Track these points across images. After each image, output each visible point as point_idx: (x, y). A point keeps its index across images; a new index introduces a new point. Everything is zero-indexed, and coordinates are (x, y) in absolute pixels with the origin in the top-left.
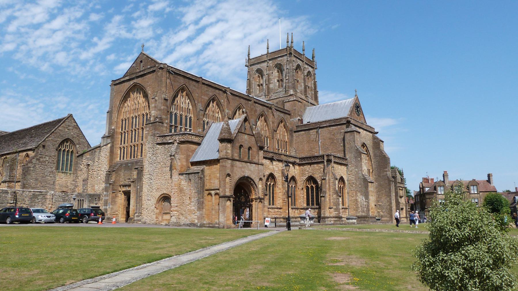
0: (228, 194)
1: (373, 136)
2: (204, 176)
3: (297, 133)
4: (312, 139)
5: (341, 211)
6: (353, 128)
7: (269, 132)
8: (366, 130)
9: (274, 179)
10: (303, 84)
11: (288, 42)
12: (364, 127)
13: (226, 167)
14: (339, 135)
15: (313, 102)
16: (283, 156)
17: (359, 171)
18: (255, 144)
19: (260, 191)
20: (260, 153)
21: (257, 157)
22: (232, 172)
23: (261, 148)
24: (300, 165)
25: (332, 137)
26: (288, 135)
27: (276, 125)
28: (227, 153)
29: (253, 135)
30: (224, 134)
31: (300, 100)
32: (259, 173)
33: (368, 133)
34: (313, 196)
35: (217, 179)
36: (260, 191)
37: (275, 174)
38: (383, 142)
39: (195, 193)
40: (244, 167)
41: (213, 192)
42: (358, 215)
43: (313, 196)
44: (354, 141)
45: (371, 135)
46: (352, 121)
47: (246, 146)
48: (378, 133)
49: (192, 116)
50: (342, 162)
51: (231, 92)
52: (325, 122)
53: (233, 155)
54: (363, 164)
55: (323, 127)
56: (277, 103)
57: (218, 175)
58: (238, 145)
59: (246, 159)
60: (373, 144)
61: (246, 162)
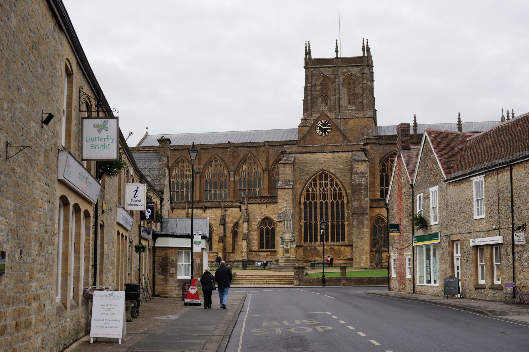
11: (306, 54)
27: (271, 163)
33: (340, 154)
45: (350, 153)
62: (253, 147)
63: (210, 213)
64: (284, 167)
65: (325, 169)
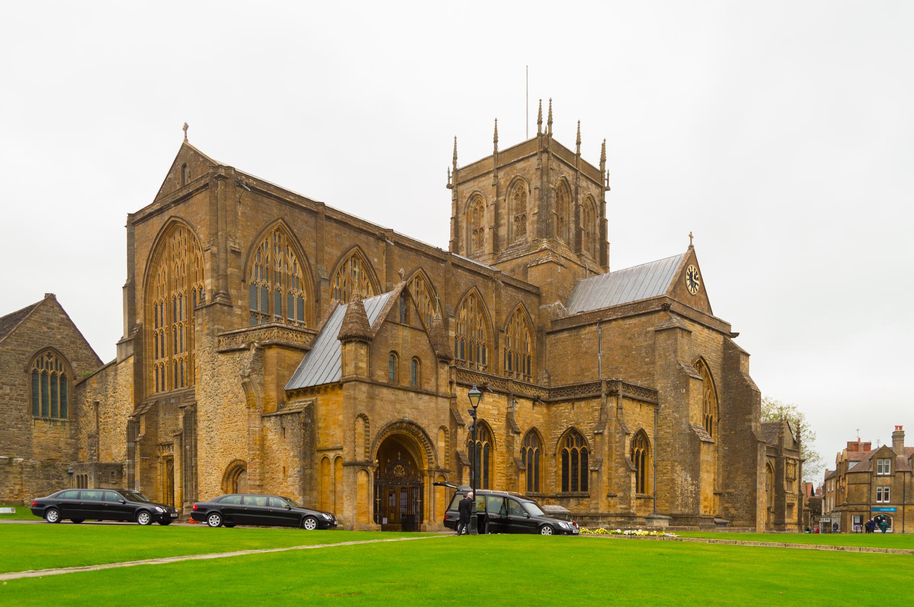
0: (360, 458)
1: (725, 340)
2: (313, 421)
3: (552, 336)
4: (584, 349)
5: (634, 503)
6: (676, 321)
7: (488, 332)
8: (708, 328)
9: (489, 432)
10: (572, 226)
12: (705, 320)
13: (355, 399)
14: (641, 339)
15: (596, 267)
16: (510, 384)
17: (681, 418)
18: (429, 352)
19: (441, 455)
20: (441, 371)
21: (433, 380)
22: (372, 410)
23: (444, 359)
24: (549, 403)
25: (627, 342)
26: (532, 342)
27: (504, 317)
28: (357, 367)
29: (424, 331)
30: (350, 325)
31: (563, 261)
32: (438, 416)
33: (714, 335)
34: (575, 470)
35: (340, 426)
36: (441, 455)
37: (490, 422)
38: (748, 355)
39: (294, 456)
40: (401, 402)
41: (331, 455)
42: (675, 512)
43: (575, 470)
44: (675, 352)
45: (720, 338)
46: (674, 306)
47: (406, 354)
48: (736, 335)
49: (305, 294)
50: (648, 396)
51: (396, 239)
52: (614, 309)
53: (371, 374)
54: (691, 402)
55: (610, 321)
56: (513, 270)
57: (341, 418)
58: (385, 351)
59: (405, 383)
60: (724, 359)
61: (406, 390)
62: (479, 274)
63: (490, 404)
64: (682, 337)
65: (704, 356)
